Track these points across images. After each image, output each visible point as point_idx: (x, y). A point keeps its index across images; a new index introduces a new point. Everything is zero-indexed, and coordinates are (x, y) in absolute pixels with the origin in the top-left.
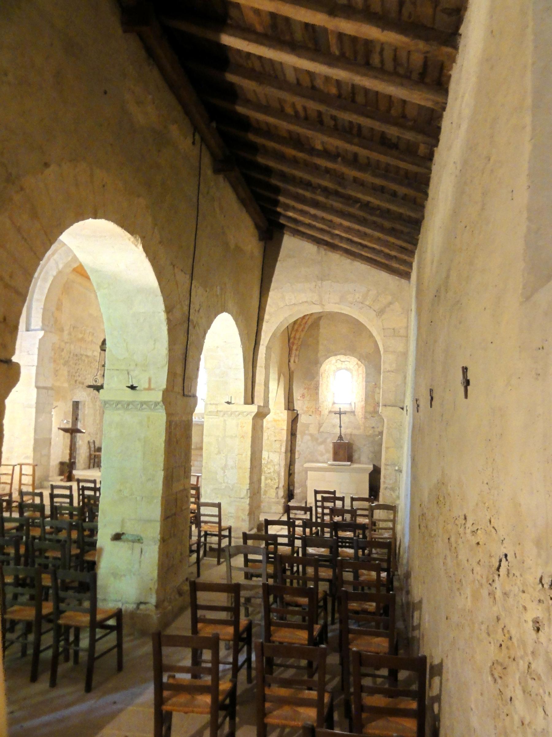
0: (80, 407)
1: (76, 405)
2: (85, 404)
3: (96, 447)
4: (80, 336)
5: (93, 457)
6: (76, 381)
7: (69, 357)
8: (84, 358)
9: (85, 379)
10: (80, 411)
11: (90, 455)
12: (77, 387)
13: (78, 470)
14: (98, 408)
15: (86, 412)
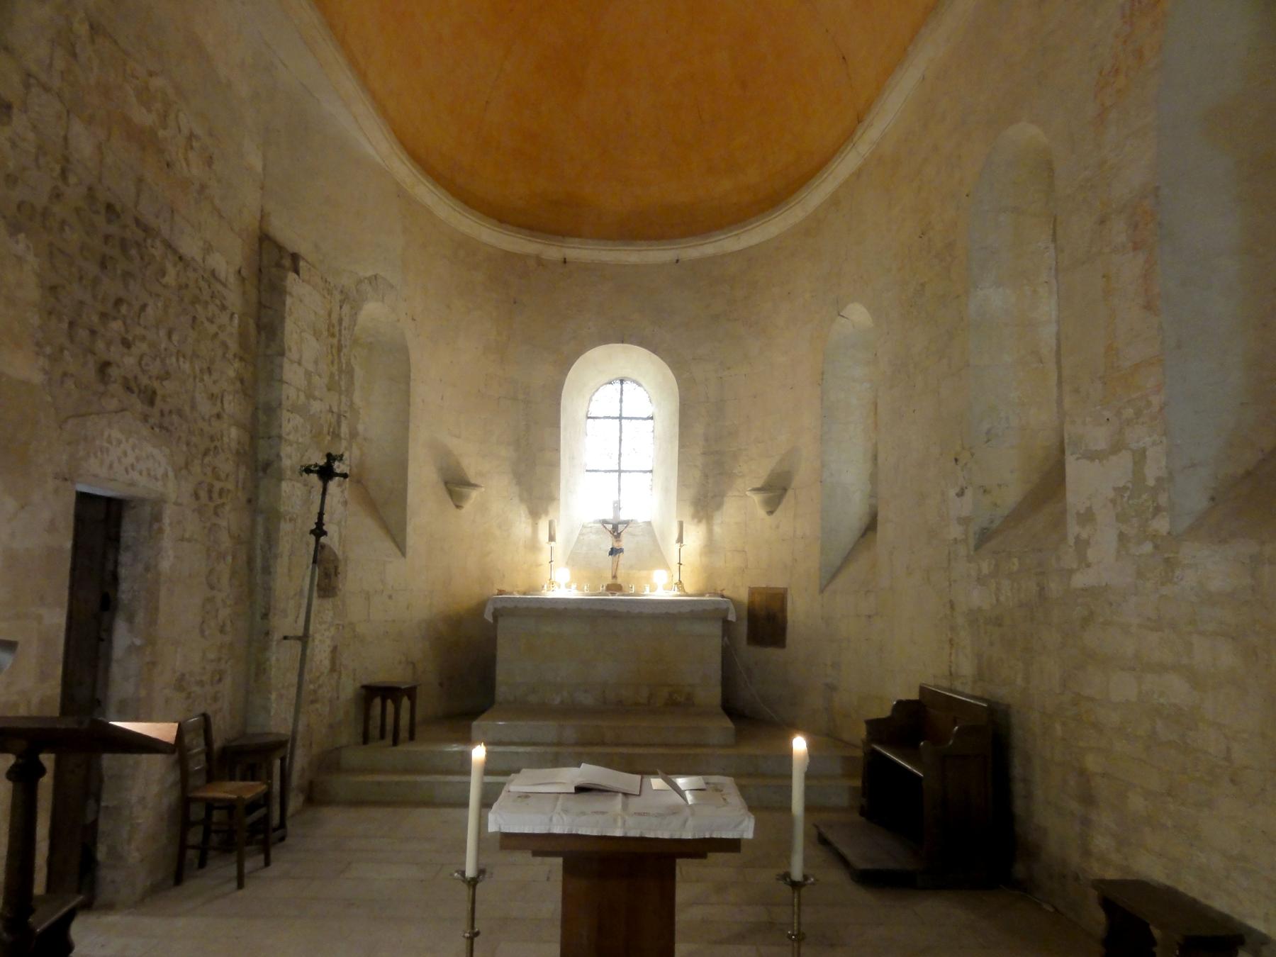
0: (128, 531)
1: (101, 526)
2: (157, 517)
3: (217, 745)
4: (143, 117)
5: (197, 812)
6: (104, 367)
7: (57, 195)
8: (157, 251)
9: (165, 376)
10: (125, 557)
11: (185, 802)
12: (113, 404)
13: (110, 907)
14: (226, 542)
15: (165, 565)
